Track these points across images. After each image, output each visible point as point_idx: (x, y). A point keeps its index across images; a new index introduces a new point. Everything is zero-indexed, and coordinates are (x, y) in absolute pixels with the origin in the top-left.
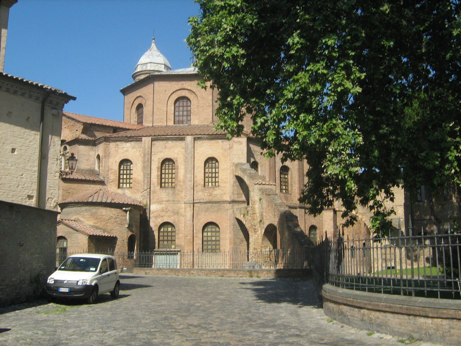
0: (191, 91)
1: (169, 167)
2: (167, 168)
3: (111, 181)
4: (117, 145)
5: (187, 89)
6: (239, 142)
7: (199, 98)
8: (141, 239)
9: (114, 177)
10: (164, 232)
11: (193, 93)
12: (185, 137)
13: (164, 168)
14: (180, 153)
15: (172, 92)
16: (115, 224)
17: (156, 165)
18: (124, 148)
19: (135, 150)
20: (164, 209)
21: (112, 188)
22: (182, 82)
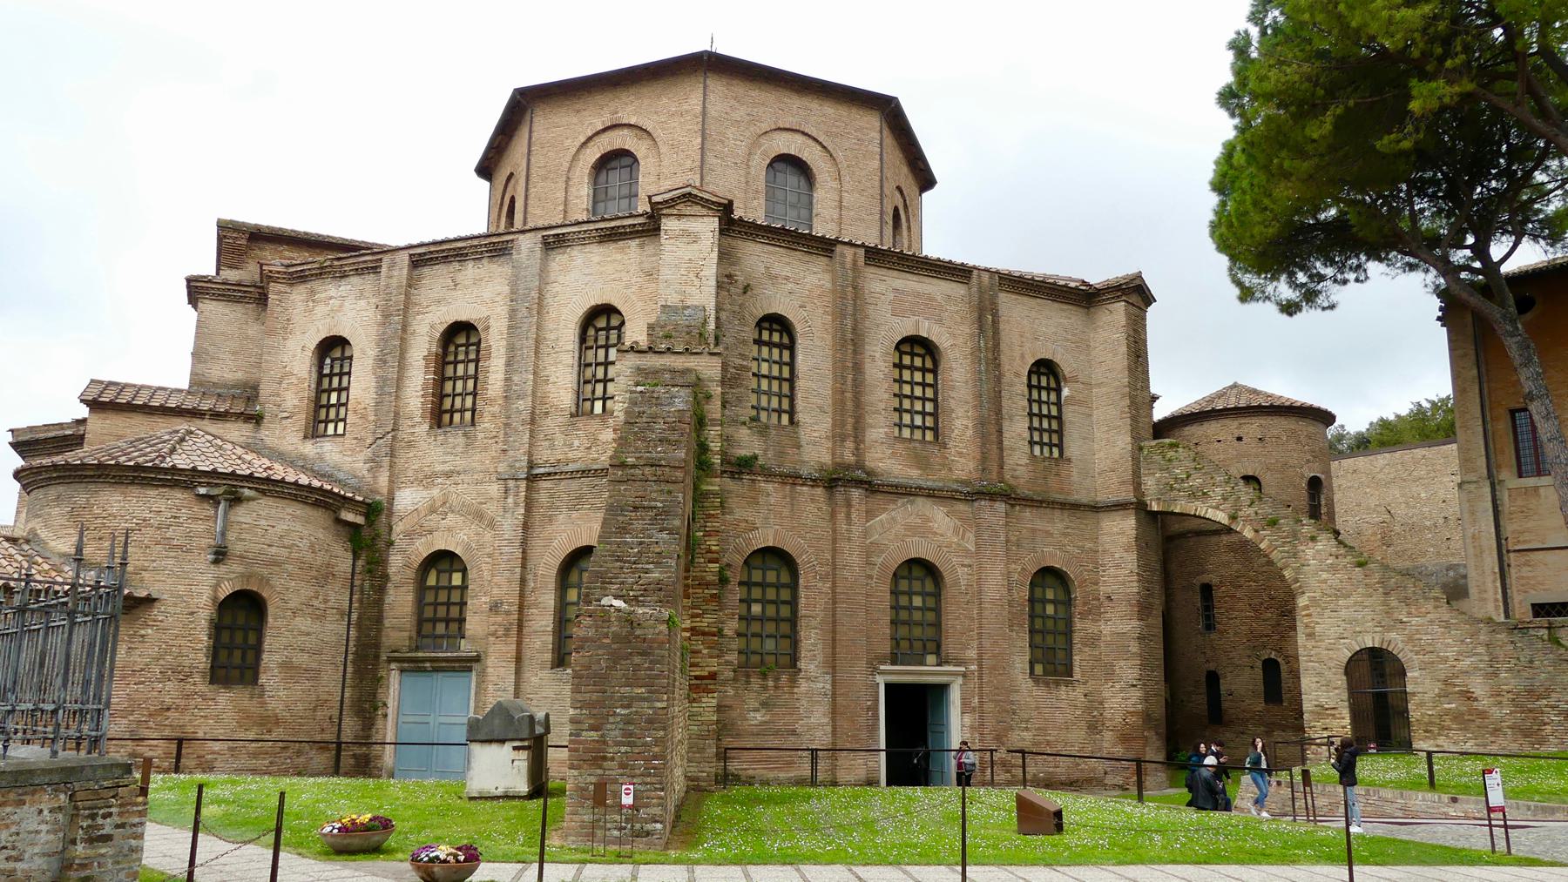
0: (641, 129)
1: (467, 353)
2: (461, 357)
3: (285, 415)
5: (630, 126)
6: (686, 233)
7: (663, 149)
8: (354, 616)
9: (296, 402)
10: (437, 588)
11: (645, 135)
12: (512, 241)
13: (451, 358)
15: (583, 140)
16: (159, 548)
17: (422, 345)
18: (331, 298)
19: (362, 303)
20: (439, 503)
21: (286, 435)
22: (613, 105)
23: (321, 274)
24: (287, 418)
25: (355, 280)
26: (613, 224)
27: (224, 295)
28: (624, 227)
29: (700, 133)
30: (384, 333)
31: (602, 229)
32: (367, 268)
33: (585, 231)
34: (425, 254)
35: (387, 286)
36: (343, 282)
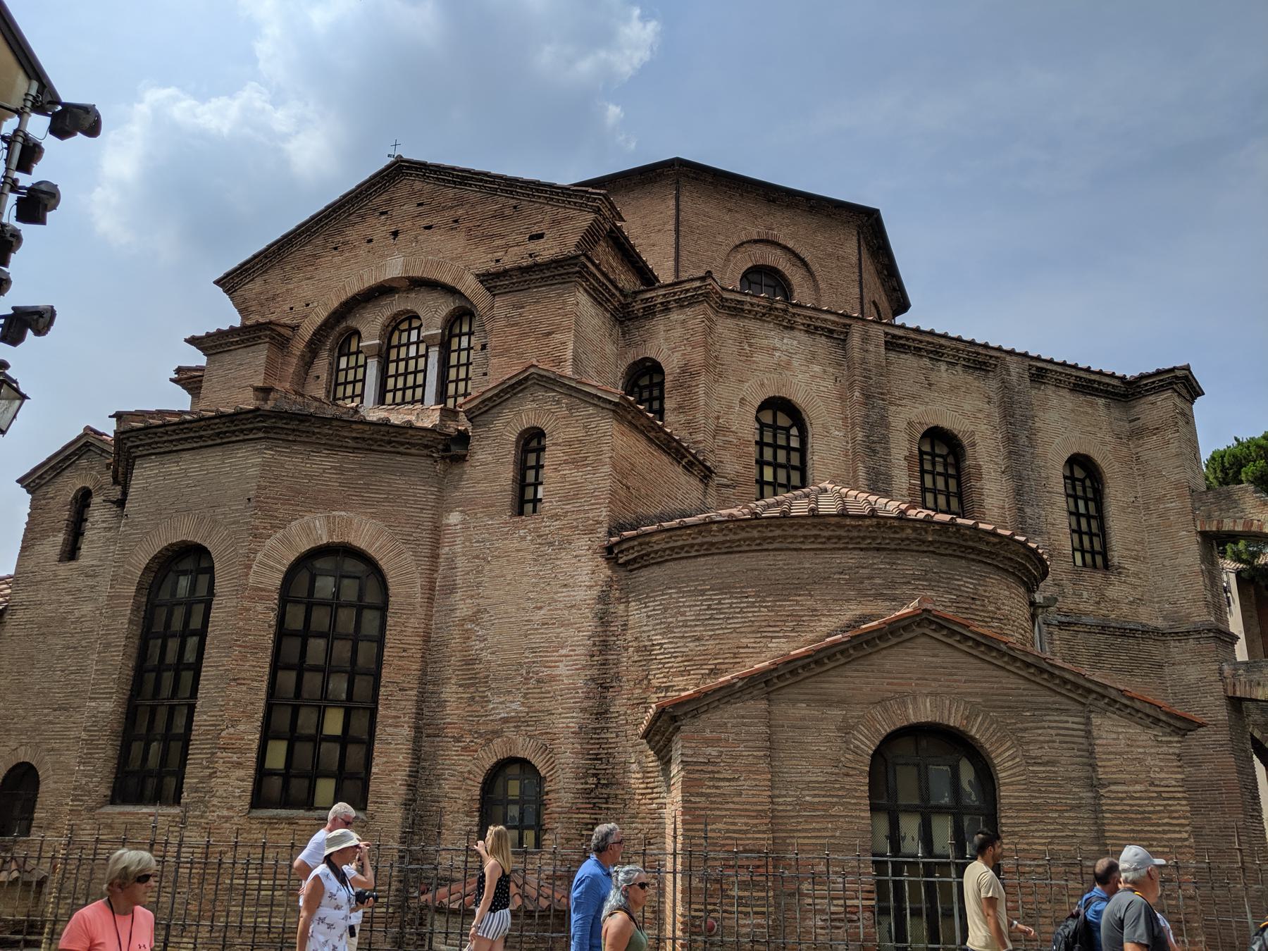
1: (934, 464)
3: (724, 481)
4: (747, 335)
5: (785, 248)
7: (822, 285)
11: (799, 263)
14: (979, 415)
18: (775, 349)
23: (764, 315)
24: (728, 486)
25: (803, 337)
26: (1093, 377)
27: (595, 289)
28: (1099, 383)
29: (857, 284)
30: (868, 416)
31: (1081, 378)
32: (823, 329)
33: (1067, 374)
34: (901, 338)
35: (864, 361)
36: (787, 334)
